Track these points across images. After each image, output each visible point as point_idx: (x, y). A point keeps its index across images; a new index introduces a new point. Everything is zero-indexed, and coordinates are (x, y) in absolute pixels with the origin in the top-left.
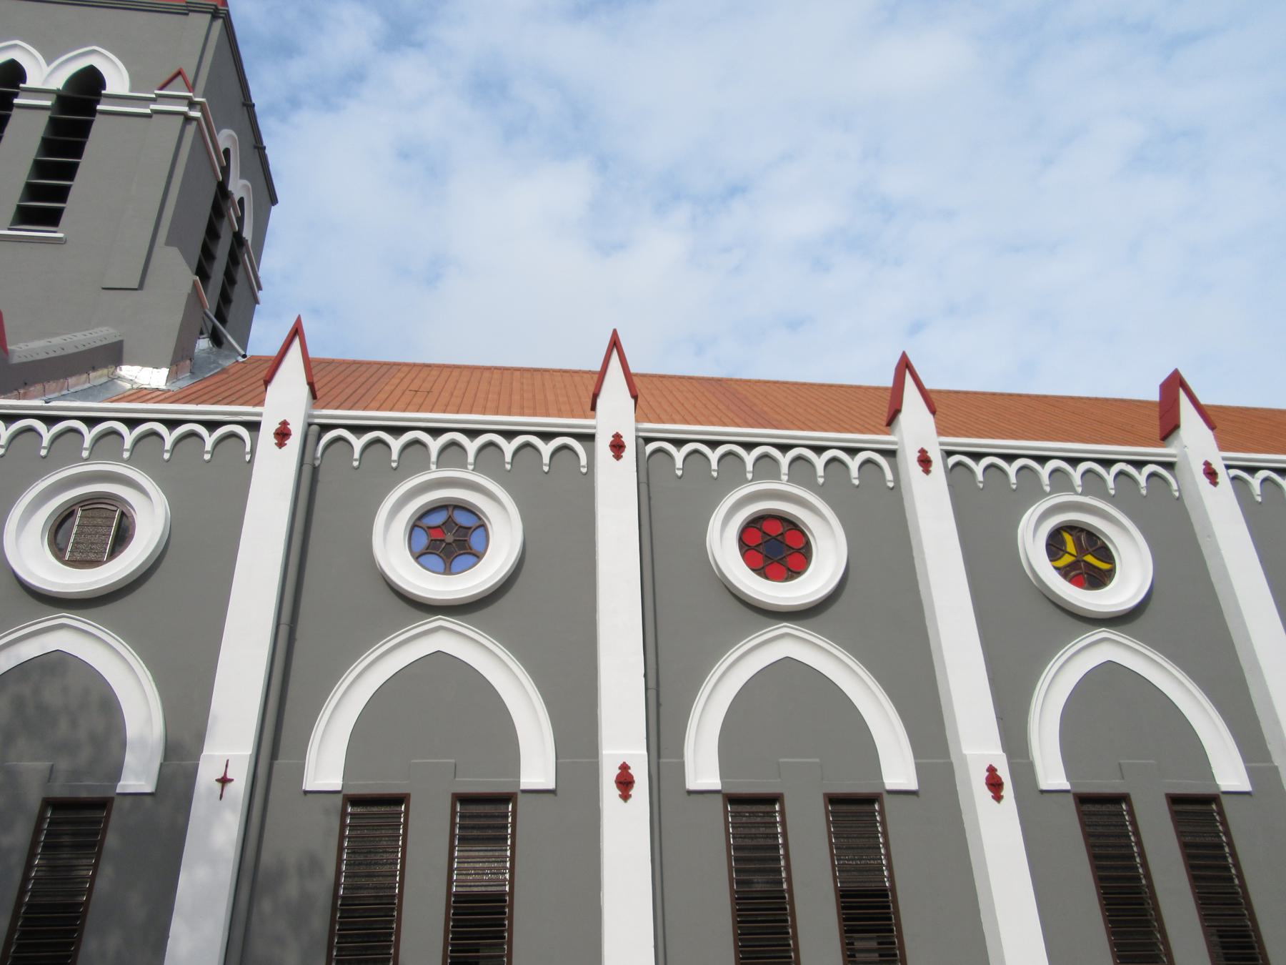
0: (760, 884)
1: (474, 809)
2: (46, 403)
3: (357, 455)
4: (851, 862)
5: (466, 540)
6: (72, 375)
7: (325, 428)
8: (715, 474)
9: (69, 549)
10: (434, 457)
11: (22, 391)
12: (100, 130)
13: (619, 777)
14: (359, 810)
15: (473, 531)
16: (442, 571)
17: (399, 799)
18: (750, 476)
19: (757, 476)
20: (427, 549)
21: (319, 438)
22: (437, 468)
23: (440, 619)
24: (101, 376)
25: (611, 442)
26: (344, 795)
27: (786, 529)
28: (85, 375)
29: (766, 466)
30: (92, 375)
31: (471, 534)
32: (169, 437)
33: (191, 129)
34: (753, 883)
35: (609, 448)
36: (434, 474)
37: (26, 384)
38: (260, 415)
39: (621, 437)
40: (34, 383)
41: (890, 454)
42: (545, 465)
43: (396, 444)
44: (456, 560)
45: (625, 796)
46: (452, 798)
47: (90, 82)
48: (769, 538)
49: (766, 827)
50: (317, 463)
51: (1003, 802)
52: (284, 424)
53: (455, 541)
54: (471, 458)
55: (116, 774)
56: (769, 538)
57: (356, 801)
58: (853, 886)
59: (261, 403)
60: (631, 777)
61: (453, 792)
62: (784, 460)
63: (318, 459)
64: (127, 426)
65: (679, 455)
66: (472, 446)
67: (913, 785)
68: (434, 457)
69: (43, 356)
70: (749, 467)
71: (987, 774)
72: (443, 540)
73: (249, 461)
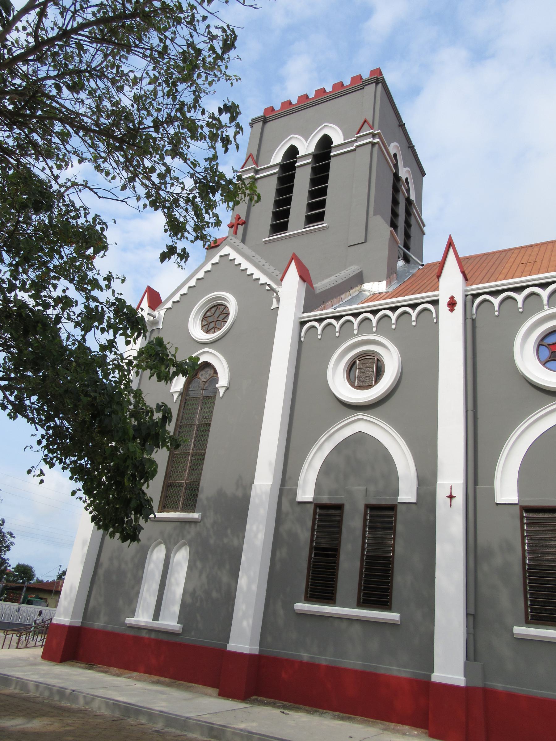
2: (335, 309)
3: (496, 308)
6: (343, 293)
7: (476, 296)
9: (356, 381)
12: (334, 164)
14: (530, 515)
21: (473, 303)
22: (548, 307)
24: (355, 291)
28: (348, 292)
30: (351, 291)
32: (394, 316)
33: (377, 146)
36: (548, 311)
38: (438, 295)
40: (327, 301)
43: (520, 298)
50: (474, 317)
52: (452, 298)
55: (396, 493)
59: (437, 289)
63: (474, 314)
69: (329, 287)
73: (436, 322)
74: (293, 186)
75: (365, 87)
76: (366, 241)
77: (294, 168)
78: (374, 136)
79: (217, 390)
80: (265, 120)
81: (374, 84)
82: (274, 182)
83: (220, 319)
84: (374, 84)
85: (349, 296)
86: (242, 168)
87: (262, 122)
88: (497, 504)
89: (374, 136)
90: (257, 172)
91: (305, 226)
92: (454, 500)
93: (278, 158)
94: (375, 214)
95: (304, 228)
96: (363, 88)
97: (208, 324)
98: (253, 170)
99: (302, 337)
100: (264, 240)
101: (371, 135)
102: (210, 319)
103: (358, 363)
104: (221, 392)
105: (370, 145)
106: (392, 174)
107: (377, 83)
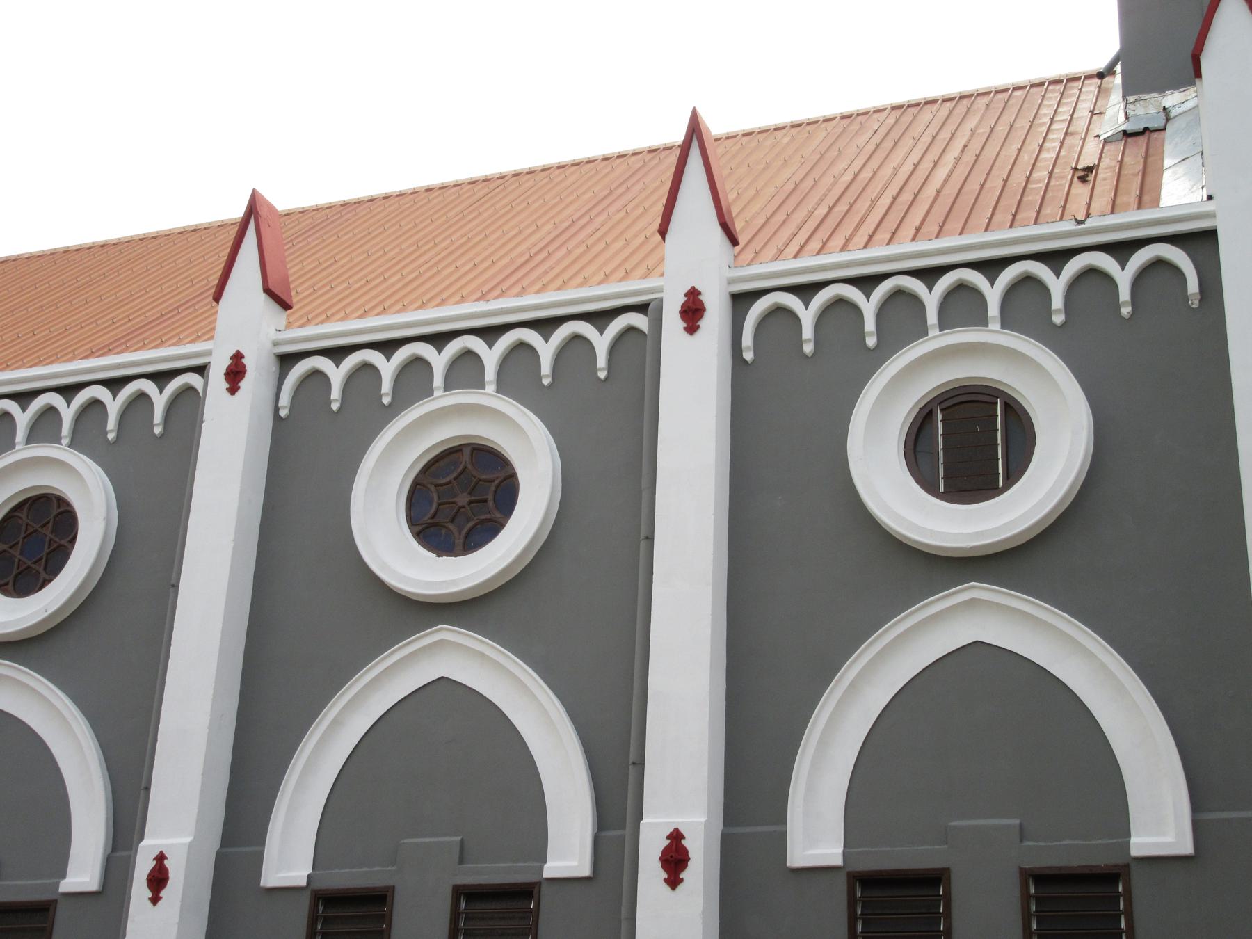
1: (479, 906)
10: (438, 380)
22: (446, 389)
23: (442, 629)
25: (683, 306)
35: (678, 316)
38: (208, 353)
39: (699, 293)
43: (387, 367)
45: (673, 881)
46: (311, 894)
53: (471, 502)
54: (490, 373)
55: (63, 875)
59: (209, 333)
64: (330, 359)
67: (1187, 848)
72: (454, 503)
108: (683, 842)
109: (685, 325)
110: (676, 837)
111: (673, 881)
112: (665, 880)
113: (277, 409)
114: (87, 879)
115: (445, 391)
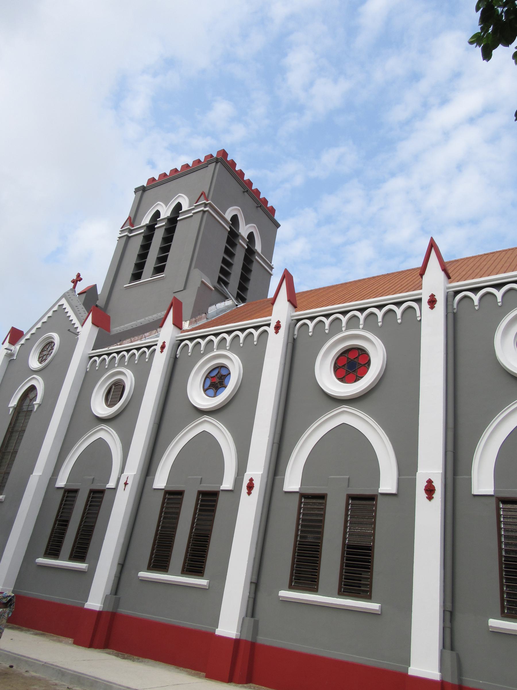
0: (310, 538)
2: (108, 348)
4: (356, 531)
5: (223, 381)
8: (327, 331)
10: (215, 346)
11: (119, 344)
12: (179, 226)
13: (426, 487)
15: (226, 377)
16: (213, 396)
17: (322, 497)
18: (344, 329)
19: (348, 328)
20: (209, 386)
21: (179, 345)
26: (165, 491)
27: (360, 354)
28: (155, 331)
29: (353, 322)
31: (225, 378)
32: (137, 354)
33: (207, 213)
34: (314, 538)
36: (216, 353)
37: (120, 340)
40: (125, 339)
41: (419, 301)
42: (255, 341)
43: (203, 343)
44: (218, 390)
47: (179, 206)
48: (351, 360)
49: (318, 511)
51: (433, 500)
52: (164, 343)
53: (219, 382)
54: (228, 344)
56: (351, 360)
57: (506, 501)
58: (355, 543)
60: (434, 487)
61: (185, 491)
62: (362, 317)
65: (311, 325)
66: (229, 338)
67: (394, 490)
68: (215, 346)
70: (344, 324)
71: (426, 484)
73: (203, 354)
74: (151, 243)
75: (209, 166)
76: (185, 288)
77: (154, 229)
78: (206, 205)
79: (33, 405)
80: (144, 189)
81: (215, 163)
82: (141, 238)
83: (50, 353)
84: (215, 163)
85: (155, 333)
86: (122, 228)
87: (142, 191)
88: (155, 489)
89: (206, 205)
90: (131, 231)
91: (152, 275)
92: (127, 486)
93: (146, 220)
94: (195, 267)
95: (151, 277)
96: (208, 166)
97: (43, 357)
98: (128, 230)
99: (97, 366)
100: (124, 286)
101: (204, 205)
102: (45, 353)
103: (113, 388)
104: (36, 407)
105: (201, 213)
106: (228, 232)
107: (217, 162)
108: (253, 482)
109: (275, 331)
110: (251, 480)
111: (249, 493)
112: (247, 492)
113: (176, 355)
114: (113, 484)
115: (217, 350)
